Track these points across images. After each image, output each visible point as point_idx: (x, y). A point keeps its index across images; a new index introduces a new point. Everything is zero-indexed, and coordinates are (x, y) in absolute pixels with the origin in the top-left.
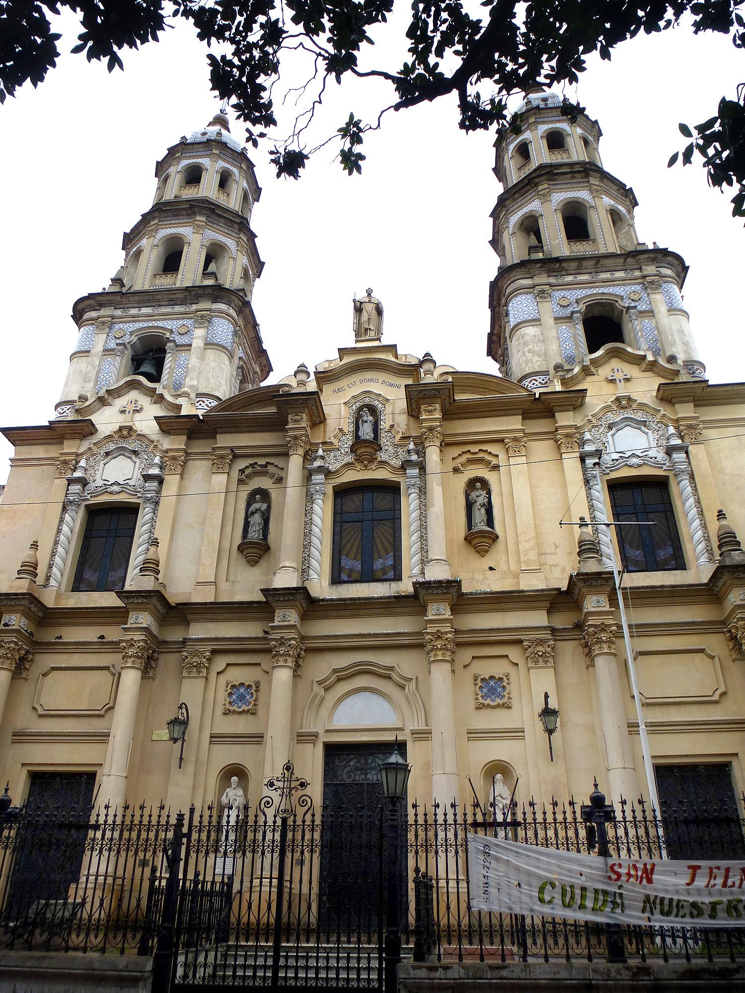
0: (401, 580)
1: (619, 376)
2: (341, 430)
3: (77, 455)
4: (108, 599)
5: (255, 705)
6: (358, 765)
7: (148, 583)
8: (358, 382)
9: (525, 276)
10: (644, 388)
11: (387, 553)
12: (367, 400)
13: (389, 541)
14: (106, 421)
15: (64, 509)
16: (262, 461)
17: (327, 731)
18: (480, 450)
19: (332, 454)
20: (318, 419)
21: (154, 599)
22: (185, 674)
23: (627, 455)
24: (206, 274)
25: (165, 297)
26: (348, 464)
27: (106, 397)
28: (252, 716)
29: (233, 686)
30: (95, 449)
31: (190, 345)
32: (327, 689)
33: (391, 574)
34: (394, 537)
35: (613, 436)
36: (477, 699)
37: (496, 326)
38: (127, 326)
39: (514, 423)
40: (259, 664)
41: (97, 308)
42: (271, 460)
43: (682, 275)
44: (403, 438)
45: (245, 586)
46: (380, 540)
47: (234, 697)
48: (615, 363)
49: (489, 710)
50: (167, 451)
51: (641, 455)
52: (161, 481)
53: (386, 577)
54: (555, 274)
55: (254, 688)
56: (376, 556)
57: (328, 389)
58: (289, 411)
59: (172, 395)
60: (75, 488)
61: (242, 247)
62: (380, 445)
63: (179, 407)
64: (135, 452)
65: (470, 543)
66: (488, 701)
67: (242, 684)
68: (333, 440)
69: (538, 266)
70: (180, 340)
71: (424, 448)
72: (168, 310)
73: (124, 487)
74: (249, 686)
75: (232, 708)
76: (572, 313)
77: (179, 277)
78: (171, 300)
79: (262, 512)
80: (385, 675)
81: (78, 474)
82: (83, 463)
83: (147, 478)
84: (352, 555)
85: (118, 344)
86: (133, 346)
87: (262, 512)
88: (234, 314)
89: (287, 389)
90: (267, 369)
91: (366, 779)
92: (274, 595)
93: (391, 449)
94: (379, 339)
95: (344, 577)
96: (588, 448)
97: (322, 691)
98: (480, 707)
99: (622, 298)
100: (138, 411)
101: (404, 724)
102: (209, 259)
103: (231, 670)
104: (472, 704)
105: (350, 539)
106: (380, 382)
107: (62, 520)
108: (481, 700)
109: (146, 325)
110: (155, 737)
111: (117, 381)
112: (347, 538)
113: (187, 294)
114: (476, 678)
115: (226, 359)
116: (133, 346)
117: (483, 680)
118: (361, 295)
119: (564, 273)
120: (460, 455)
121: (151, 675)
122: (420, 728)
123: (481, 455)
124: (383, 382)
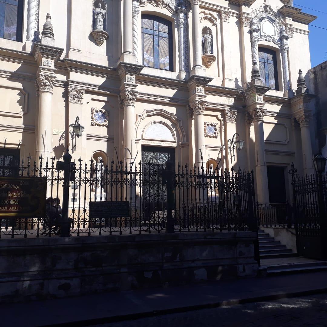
11: (166, 56)
18: (210, 14)
22: (71, 100)
23: (267, 35)
33: (168, 68)
47: (97, 117)
51: (272, 36)
53: (165, 68)
75: (97, 123)
79: (103, 15)
87: (103, 15)
96: (255, 27)
97: (141, 119)
105: (148, 44)
110: (55, 133)
122: (184, 142)
123: (208, 16)
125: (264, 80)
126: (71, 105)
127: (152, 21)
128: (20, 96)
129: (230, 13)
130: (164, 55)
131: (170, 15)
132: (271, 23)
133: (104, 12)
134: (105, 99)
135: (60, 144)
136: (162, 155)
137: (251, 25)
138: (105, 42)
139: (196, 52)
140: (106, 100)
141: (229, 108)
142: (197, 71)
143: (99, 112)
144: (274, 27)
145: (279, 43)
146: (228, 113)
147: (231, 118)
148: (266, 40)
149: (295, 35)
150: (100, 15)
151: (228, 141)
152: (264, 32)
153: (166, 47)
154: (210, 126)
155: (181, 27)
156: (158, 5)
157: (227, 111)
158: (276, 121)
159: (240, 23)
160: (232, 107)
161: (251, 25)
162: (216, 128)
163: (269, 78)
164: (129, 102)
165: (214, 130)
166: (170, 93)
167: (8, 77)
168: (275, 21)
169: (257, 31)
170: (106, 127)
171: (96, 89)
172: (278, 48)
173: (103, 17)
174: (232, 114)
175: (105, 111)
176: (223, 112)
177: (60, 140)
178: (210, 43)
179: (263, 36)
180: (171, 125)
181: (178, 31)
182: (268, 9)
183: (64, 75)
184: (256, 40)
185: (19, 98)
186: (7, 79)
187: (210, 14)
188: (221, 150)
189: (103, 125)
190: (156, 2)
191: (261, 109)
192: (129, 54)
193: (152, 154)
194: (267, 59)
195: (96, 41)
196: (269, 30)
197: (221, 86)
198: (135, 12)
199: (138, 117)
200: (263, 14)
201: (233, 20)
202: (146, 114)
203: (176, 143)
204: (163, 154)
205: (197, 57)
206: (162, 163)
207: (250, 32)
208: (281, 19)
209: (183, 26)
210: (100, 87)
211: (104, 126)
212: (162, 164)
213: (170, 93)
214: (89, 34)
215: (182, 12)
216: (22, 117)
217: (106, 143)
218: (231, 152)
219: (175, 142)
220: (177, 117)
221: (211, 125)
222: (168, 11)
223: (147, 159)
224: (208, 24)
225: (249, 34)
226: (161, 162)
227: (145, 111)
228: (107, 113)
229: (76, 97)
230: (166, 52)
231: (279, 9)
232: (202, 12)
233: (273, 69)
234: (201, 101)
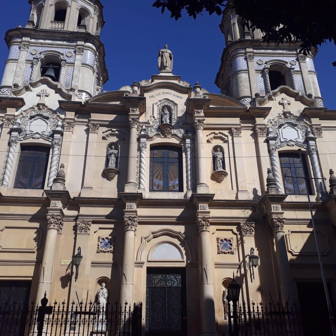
1: (285, 102)
2: (154, 117)
3: (14, 116)
4: (37, 193)
6: (163, 278)
7: (58, 187)
8: (161, 94)
9: (242, 47)
10: (296, 108)
11: (175, 179)
12: (166, 104)
14: (30, 98)
15: (9, 144)
17: (148, 262)
18: (220, 133)
19: (149, 129)
20: (143, 111)
21: (64, 196)
22: (78, 232)
23: (288, 140)
24: (79, 24)
27: (30, 86)
30: (24, 113)
31: (74, 64)
33: (177, 188)
35: (281, 130)
37: (223, 70)
38: (38, 48)
39: (237, 121)
41: (21, 36)
43: (314, 54)
45: (109, 190)
47: (103, 244)
48: (284, 95)
50: (64, 119)
51: (294, 140)
52: (62, 135)
53: (175, 189)
54: (256, 48)
56: (170, 179)
57: (146, 95)
59: (66, 90)
60: (15, 134)
61: (97, 12)
63: (70, 97)
64: (47, 118)
66: (224, 250)
68: (150, 122)
69: (249, 43)
70: (68, 61)
71: (195, 131)
73: (42, 136)
75: (102, 250)
76: (265, 68)
77: (66, 24)
78: (62, 37)
79: (115, 154)
81: (15, 127)
82: (18, 121)
83: (55, 132)
85: (34, 58)
86: (42, 60)
87: (115, 154)
88: (96, 50)
89: (127, 94)
90: (106, 79)
95: (155, 188)
96: (270, 135)
97: (146, 242)
99: (287, 63)
100: (47, 96)
102: (81, 18)
106: (172, 94)
107: (9, 151)
109: (49, 49)
110: (62, 263)
111: (37, 79)
112: (156, 170)
114: (218, 239)
115: (91, 72)
116: (42, 60)
117: (222, 240)
119: (261, 48)
120: (210, 134)
121: (60, 232)
123: (219, 135)
124: (174, 95)
125: (291, 185)
126: (78, 236)
127: (163, 150)
128: (36, 234)
129: (241, 128)
131: (177, 142)
132: (292, 127)
133: (116, 152)
134: (112, 226)
135: (67, 274)
136: (171, 276)
137: (267, 134)
138: (116, 176)
139: (199, 172)
140: (113, 227)
141: (245, 220)
142: (199, 189)
143: (105, 239)
144: (297, 131)
145: (305, 146)
146: (243, 226)
147: (247, 231)
148: (288, 145)
149: (325, 133)
150: (112, 155)
151: (246, 256)
152: (284, 138)
153: (176, 170)
154: (225, 242)
155: (188, 151)
156: (165, 137)
157: (242, 224)
158: (311, 230)
159: (255, 136)
160: (249, 220)
161: (267, 134)
162: (231, 243)
163: (297, 183)
164: (127, 227)
165: (229, 245)
166: (177, 212)
167: (29, 219)
168: (297, 125)
169: (274, 139)
170: (111, 252)
171: (104, 219)
172: (305, 150)
173: (116, 156)
174: (248, 226)
175: (111, 238)
176: (238, 224)
177: (67, 270)
178: (221, 159)
179: (283, 142)
180: (180, 244)
181: (186, 155)
182: (287, 115)
183: (76, 211)
184: (273, 147)
185: (35, 235)
186: (28, 221)
187: (220, 133)
188: (240, 268)
189: (108, 252)
190: (163, 134)
191: (279, 219)
192: (129, 184)
193: (160, 277)
194: (294, 164)
195: (108, 177)
196: (292, 135)
197: (234, 199)
198: (143, 147)
199: (143, 239)
200: (283, 120)
201: (246, 134)
202: (152, 236)
203: (186, 263)
204: (173, 276)
205: (200, 176)
206: (172, 285)
207: (267, 141)
208: (305, 121)
209: (189, 150)
210: (107, 217)
211: (109, 252)
212: (172, 287)
213: (177, 212)
214: (102, 172)
215: (188, 138)
216: (36, 252)
217: (111, 268)
218: (250, 269)
219: (184, 262)
220: (184, 236)
221: (226, 239)
222: (175, 139)
223: (154, 282)
224: (219, 142)
225: (266, 144)
226: (170, 285)
227: (151, 232)
228: (112, 239)
229: (84, 229)
230: (175, 173)
231: (301, 112)
232: (212, 133)
233: (302, 172)
234: (204, 217)
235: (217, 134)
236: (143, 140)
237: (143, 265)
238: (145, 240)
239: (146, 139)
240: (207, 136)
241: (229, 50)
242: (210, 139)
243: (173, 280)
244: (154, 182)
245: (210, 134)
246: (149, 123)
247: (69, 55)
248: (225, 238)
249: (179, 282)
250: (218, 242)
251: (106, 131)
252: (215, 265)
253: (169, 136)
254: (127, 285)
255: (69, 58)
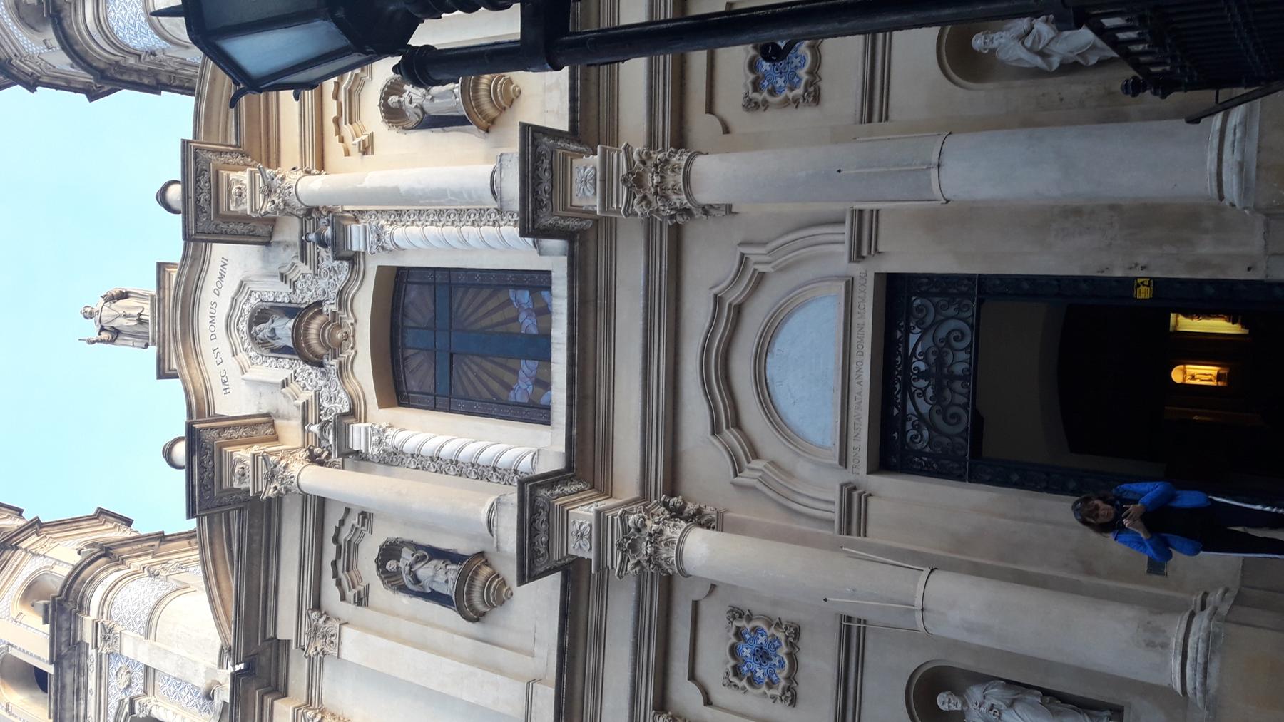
0: (549, 273)
2: (285, 384)
5: (778, 625)
11: (509, 302)
12: (244, 327)
13: (491, 297)
16: (330, 551)
17: (844, 460)
18: (336, 96)
19: (325, 405)
25: (68, 705)
26: (341, 371)
28: (805, 636)
29: (737, 671)
31: (147, 667)
32: (755, 455)
34: (481, 286)
36: (796, 102)
40: (696, 605)
42: (330, 532)
44: (303, 258)
46: (485, 316)
47: (759, 673)
49: (825, 71)
55: (742, 623)
56: (513, 327)
58: (226, 484)
62: (309, 307)
65: (493, 122)
66: (803, 73)
67: (733, 651)
68: (300, 402)
72: (92, 699)
74: (739, 634)
75: (783, 683)
79: (417, 561)
80: (730, 315)
84: (508, 377)
87: (417, 561)
91: (963, 378)
92: (534, 555)
93: (323, 283)
94: (153, 297)
97: (756, 464)
98: (814, 95)
101: (839, 278)
103: (701, 671)
104: (807, 114)
106: (215, 298)
108: (799, 91)
113: (65, 663)
114: (751, 105)
117: (756, 86)
118: (92, 329)
120: (342, 140)
122: (846, 238)
124: (217, 292)
130: (508, 313)
173: (424, 557)
202: (730, 435)
227: (712, 438)
232: (338, 132)
235: (339, 106)
236: (358, 437)
237: (855, 494)
238: (746, 472)
239: (356, 426)
240: (347, 153)
241: (102, 66)
242: (357, 140)
243: (942, 340)
244: (526, 400)
245: (342, 140)
246: (305, 406)
247: (124, 680)
248: (747, 72)
249: (951, 312)
250: (766, 104)
251: (339, 584)
252: (870, 121)
253: (349, 322)
254: (928, 605)
255: (135, 681)
